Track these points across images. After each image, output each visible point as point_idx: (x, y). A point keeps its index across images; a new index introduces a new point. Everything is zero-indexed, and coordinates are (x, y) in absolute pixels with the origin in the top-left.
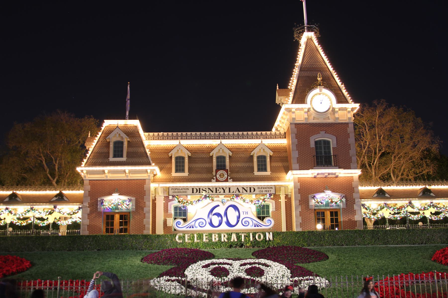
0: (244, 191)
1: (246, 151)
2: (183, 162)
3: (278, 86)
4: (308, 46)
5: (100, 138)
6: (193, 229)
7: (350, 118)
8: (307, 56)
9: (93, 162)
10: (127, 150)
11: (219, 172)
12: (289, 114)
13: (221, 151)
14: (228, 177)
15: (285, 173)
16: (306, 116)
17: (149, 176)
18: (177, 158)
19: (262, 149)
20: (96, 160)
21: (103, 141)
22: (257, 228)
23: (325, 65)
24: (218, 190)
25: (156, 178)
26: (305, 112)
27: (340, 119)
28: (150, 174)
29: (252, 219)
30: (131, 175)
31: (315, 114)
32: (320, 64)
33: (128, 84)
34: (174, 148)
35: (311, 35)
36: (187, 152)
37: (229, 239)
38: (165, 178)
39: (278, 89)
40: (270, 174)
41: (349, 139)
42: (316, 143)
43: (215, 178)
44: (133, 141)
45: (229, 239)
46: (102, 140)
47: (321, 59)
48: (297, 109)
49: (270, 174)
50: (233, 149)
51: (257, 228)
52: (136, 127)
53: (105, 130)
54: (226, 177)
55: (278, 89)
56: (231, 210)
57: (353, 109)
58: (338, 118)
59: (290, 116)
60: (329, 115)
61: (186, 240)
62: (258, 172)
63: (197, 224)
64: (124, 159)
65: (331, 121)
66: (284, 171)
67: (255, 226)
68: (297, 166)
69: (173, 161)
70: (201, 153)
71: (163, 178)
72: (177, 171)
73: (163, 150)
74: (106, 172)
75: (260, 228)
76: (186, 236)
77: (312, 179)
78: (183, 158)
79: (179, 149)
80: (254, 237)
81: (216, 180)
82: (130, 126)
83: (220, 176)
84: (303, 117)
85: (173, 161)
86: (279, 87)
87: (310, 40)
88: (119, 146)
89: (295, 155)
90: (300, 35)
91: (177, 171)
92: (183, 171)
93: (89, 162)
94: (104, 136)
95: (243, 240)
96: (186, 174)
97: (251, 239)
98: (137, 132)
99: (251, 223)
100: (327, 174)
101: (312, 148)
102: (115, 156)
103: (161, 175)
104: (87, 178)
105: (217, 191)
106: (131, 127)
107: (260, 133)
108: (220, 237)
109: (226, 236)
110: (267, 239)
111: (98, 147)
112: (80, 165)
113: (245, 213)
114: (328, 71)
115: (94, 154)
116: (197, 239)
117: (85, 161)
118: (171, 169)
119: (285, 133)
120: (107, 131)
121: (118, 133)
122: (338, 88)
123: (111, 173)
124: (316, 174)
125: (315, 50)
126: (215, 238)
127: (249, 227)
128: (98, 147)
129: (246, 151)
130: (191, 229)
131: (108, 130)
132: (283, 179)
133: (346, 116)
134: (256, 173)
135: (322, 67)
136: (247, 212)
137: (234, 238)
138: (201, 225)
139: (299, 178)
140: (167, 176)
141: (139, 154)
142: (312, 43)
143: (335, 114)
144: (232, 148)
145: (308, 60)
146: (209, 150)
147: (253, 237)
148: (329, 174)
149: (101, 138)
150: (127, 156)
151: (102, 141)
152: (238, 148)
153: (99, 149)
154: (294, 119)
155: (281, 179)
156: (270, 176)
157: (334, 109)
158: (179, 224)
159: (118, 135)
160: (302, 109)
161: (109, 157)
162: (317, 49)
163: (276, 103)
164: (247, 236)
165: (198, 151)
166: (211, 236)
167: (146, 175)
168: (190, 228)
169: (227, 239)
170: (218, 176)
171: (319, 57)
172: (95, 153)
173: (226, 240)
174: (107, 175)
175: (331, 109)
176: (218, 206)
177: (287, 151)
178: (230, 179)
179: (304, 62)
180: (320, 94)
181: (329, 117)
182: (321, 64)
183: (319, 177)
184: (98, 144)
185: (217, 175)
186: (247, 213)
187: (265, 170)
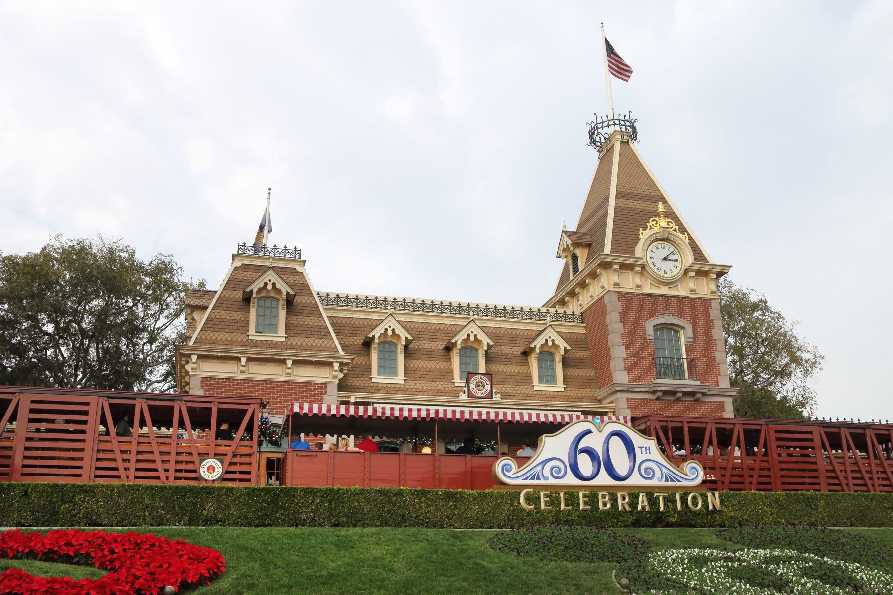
11: (474, 377)
19: (551, 339)
37: (633, 504)
43: (466, 389)
45: (633, 504)
54: (489, 388)
56: (616, 440)
61: (543, 506)
63: (547, 472)
67: (667, 480)
75: (676, 484)
83: (476, 386)
97: (679, 508)
99: (658, 474)
108: (614, 501)
110: (711, 508)
113: (644, 450)
116: (566, 505)
121: (270, 280)
127: (654, 482)
136: (648, 448)
137: (643, 502)
147: (682, 503)
158: (508, 471)
164: (670, 500)
168: (533, 479)
170: (472, 386)
173: (627, 508)
185: (471, 385)
186: (648, 451)
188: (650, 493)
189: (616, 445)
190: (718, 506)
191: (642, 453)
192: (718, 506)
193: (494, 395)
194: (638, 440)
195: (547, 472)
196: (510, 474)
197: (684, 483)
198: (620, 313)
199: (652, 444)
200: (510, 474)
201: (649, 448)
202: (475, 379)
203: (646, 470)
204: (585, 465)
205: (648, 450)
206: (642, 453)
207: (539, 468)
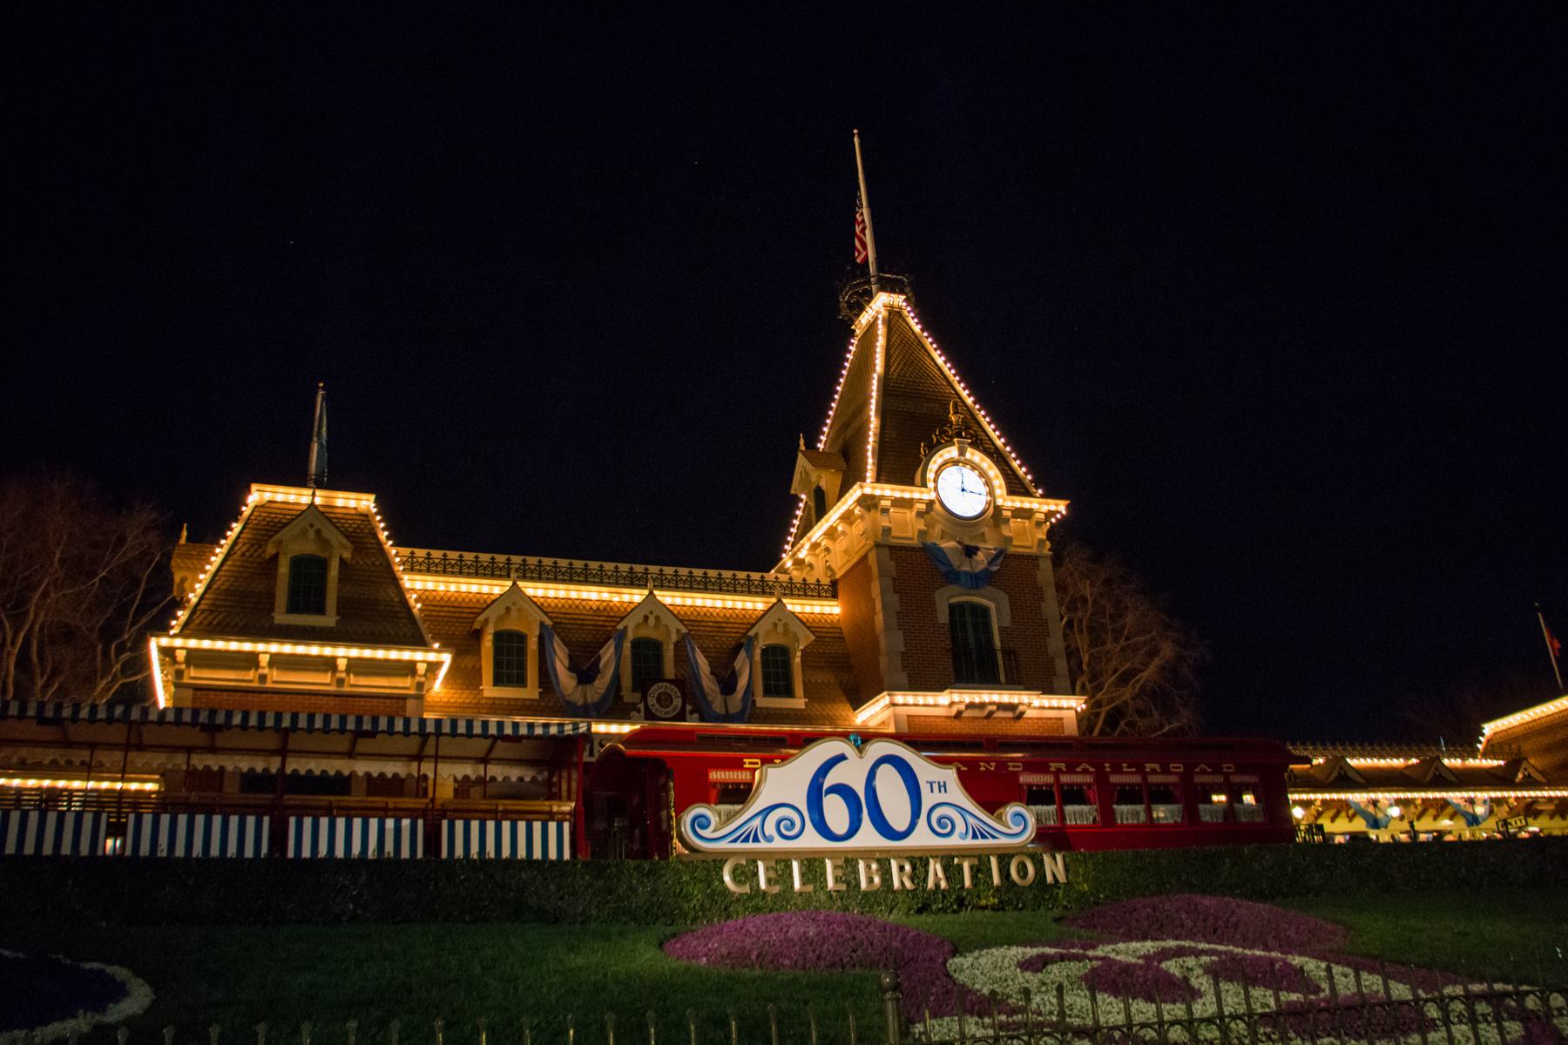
1: (720, 630)
3: (802, 442)
5: (235, 543)
6: (756, 845)
7: (1041, 542)
9: (210, 623)
10: (340, 590)
11: (656, 686)
12: (867, 516)
14: (683, 707)
15: (848, 706)
16: (921, 525)
18: (498, 636)
20: (224, 618)
21: (248, 554)
22: (980, 842)
26: (920, 514)
27: (1015, 543)
28: (423, 679)
29: (963, 812)
30: (353, 679)
31: (947, 520)
32: (937, 384)
33: (319, 387)
34: (488, 606)
35: (898, 300)
36: (538, 618)
38: (460, 700)
39: (803, 448)
40: (803, 707)
41: (1043, 604)
42: (952, 607)
43: (641, 706)
44: (358, 562)
46: (244, 549)
48: (900, 503)
49: (803, 707)
51: (980, 842)
52: (365, 518)
53: (253, 517)
54: (680, 704)
55: (803, 448)
56: (886, 771)
57: (1050, 514)
58: (1009, 540)
59: (874, 522)
60: (986, 530)
61: (763, 885)
62: (764, 696)
63: (770, 829)
64: (329, 620)
66: (844, 698)
67: (975, 836)
68: (903, 677)
69: (488, 642)
70: (574, 627)
71: (453, 700)
72: (498, 681)
73: (446, 609)
74: (264, 659)
75: (990, 842)
76: (761, 865)
77: (948, 722)
79: (511, 605)
80: (1005, 874)
81: (646, 714)
82: (345, 511)
83: (659, 700)
84: (910, 528)
85: (488, 642)
86: (805, 445)
87: (894, 316)
88: (308, 574)
89: (891, 643)
91: (498, 681)
92: (521, 681)
93: (197, 622)
94: (250, 536)
95: (967, 882)
97: (996, 880)
98: (370, 533)
99: (960, 827)
100: (995, 707)
101: (943, 624)
102: (293, 608)
103: (446, 691)
106: (346, 517)
107: (759, 579)
109: (908, 867)
110: (1049, 879)
111: (231, 574)
112: (162, 628)
113: (936, 787)
115: (212, 596)
117: (182, 615)
119: (834, 583)
120: (262, 523)
123: (278, 668)
124: (962, 707)
126: (867, 879)
127: (954, 841)
128: (228, 573)
129: (720, 630)
130: (750, 845)
131: (263, 520)
134: (763, 702)
136: (942, 784)
138: (787, 829)
139: (911, 718)
140: (464, 696)
141: (381, 608)
145: (902, 369)
146: (601, 618)
149: (240, 545)
150: (340, 610)
151: (243, 555)
153: (231, 579)
154: (887, 531)
156: (805, 713)
157: (998, 509)
159: (311, 534)
161: (272, 610)
162: (920, 341)
163: (792, 492)
164: (981, 870)
165: (564, 618)
166: (856, 872)
167: (408, 682)
168: (746, 840)
169: (912, 879)
170: (652, 701)
172: (218, 591)
173: (908, 884)
176: (841, 758)
177: (843, 638)
178: (692, 713)
180: (955, 463)
181: (983, 533)
182: (938, 382)
183: (968, 718)
184: (229, 563)
185: (649, 699)
186: (942, 789)
187: (789, 693)
188: (948, 859)
189: (888, 780)
190: (1062, 878)
191: (932, 791)
192: (1062, 878)
193: (688, 716)
194: (924, 769)
195: (770, 829)
196: (706, 833)
197: (1003, 841)
198: (894, 579)
199: (950, 775)
200: (706, 833)
201: (945, 783)
202: (656, 690)
203: (939, 821)
204: (836, 812)
205: (943, 787)
206: (932, 791)
207: (757, 822)
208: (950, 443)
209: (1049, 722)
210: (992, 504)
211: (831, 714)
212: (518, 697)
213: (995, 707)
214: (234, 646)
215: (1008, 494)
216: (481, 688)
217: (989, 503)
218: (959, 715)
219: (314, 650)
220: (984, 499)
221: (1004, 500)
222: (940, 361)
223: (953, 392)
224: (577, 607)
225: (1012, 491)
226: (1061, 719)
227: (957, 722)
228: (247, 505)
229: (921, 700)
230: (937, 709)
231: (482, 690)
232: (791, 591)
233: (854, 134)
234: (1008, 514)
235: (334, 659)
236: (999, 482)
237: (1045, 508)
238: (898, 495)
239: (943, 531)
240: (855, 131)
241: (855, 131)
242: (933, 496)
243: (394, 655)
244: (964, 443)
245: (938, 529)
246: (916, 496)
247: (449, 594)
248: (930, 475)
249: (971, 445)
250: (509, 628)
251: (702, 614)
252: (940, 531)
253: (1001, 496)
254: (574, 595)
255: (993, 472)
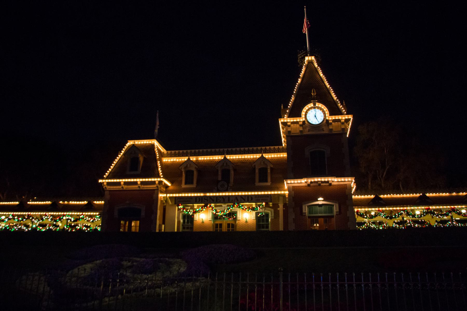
0: (242, 199)
2: (193, 175)
3: (282, 106)
4: (308, 68)
8: (306, 76)
13: (225, 165)
16: (301, 129)
17: (157, 187)
23: (323, 83)
24: (219, 199)
25: (169, 189)
26: (300, 125)
27: (334, 130)
32: (319, 83)
47: (319, 78)
48: (293, 123)
50: (239, 163)
58: (332, 129)
59: (287, 129)
60: (324, 127)
64: (139, 172)
65: (326, 132)
72: (186, 183)
74: (122, 183)
78: (192, 172)
84: (298, 130)
86: (283, 107)
88: (135, 161)
90: (302, 60)
91: (186, 183)
92: (192, 183)
96: (194, 186)
100: (320, 182)
104: (107, 189)
105: (218, 200)
114: (325, 88)
118: (181, 181)
122: (332, 100)
125: (315, 71)
132: (282, 189)
133: (340, 127)
134: (257, 184)
135: (320, 85)
142: (313, 65)
143: (329, 126)
144: (238, 162)
148: (322, 182)
152: (243, 162)
155: (280, 189)
157: (327, 121)
160: (297, 123)
171: (317, 76)
174: (123, 186)
175: (325, 121)
178: (230, 189)
179: (303, 82)
180: (314, 108)
181: (323, 129)
182: (319, 82)
183: (313, 186)
187: (266, 181)
193: (229, 190)
208: (311, 102)
209: (342, 186)
210: (325, 119)
211: (278, 186)
212: (191, 187)
213: (320, 182)
214: (115, 181)
215: (330, 115)
216: (181, 185)
217: (324, 119)
218: (309, 185)
219: (132, 180)
220: (322, 118)
221: (329, 118)
222: (321, 75)
223: (323, 84)
224: (212, 162)
225: (331, 114)
226: (346, 185)
227: (309, 187)
228: (126, 146)
229: (296, 182)
230: (345, 182)
231: (182, 186)
232: (283, 151)
233: (304, 8)
234: (331, 121)
235: (137, 182)
236: (327, 112)
237: (344, 118)
238: (292, 121)
239: (309, 129)
240: (305, 7)
241: (305, 7)
242: (304, 119)
243: (150, 180)
244: (315, 102)
245: (308, 129)
246: (298, 120)
247: (179, 162)
248: (303, 113)
249: (317, 102)
250: (192, 169)
251: (246, 160)
252: (308, 130)
253: (328, 116)
254: (211, 158)
255: (326, 109)
